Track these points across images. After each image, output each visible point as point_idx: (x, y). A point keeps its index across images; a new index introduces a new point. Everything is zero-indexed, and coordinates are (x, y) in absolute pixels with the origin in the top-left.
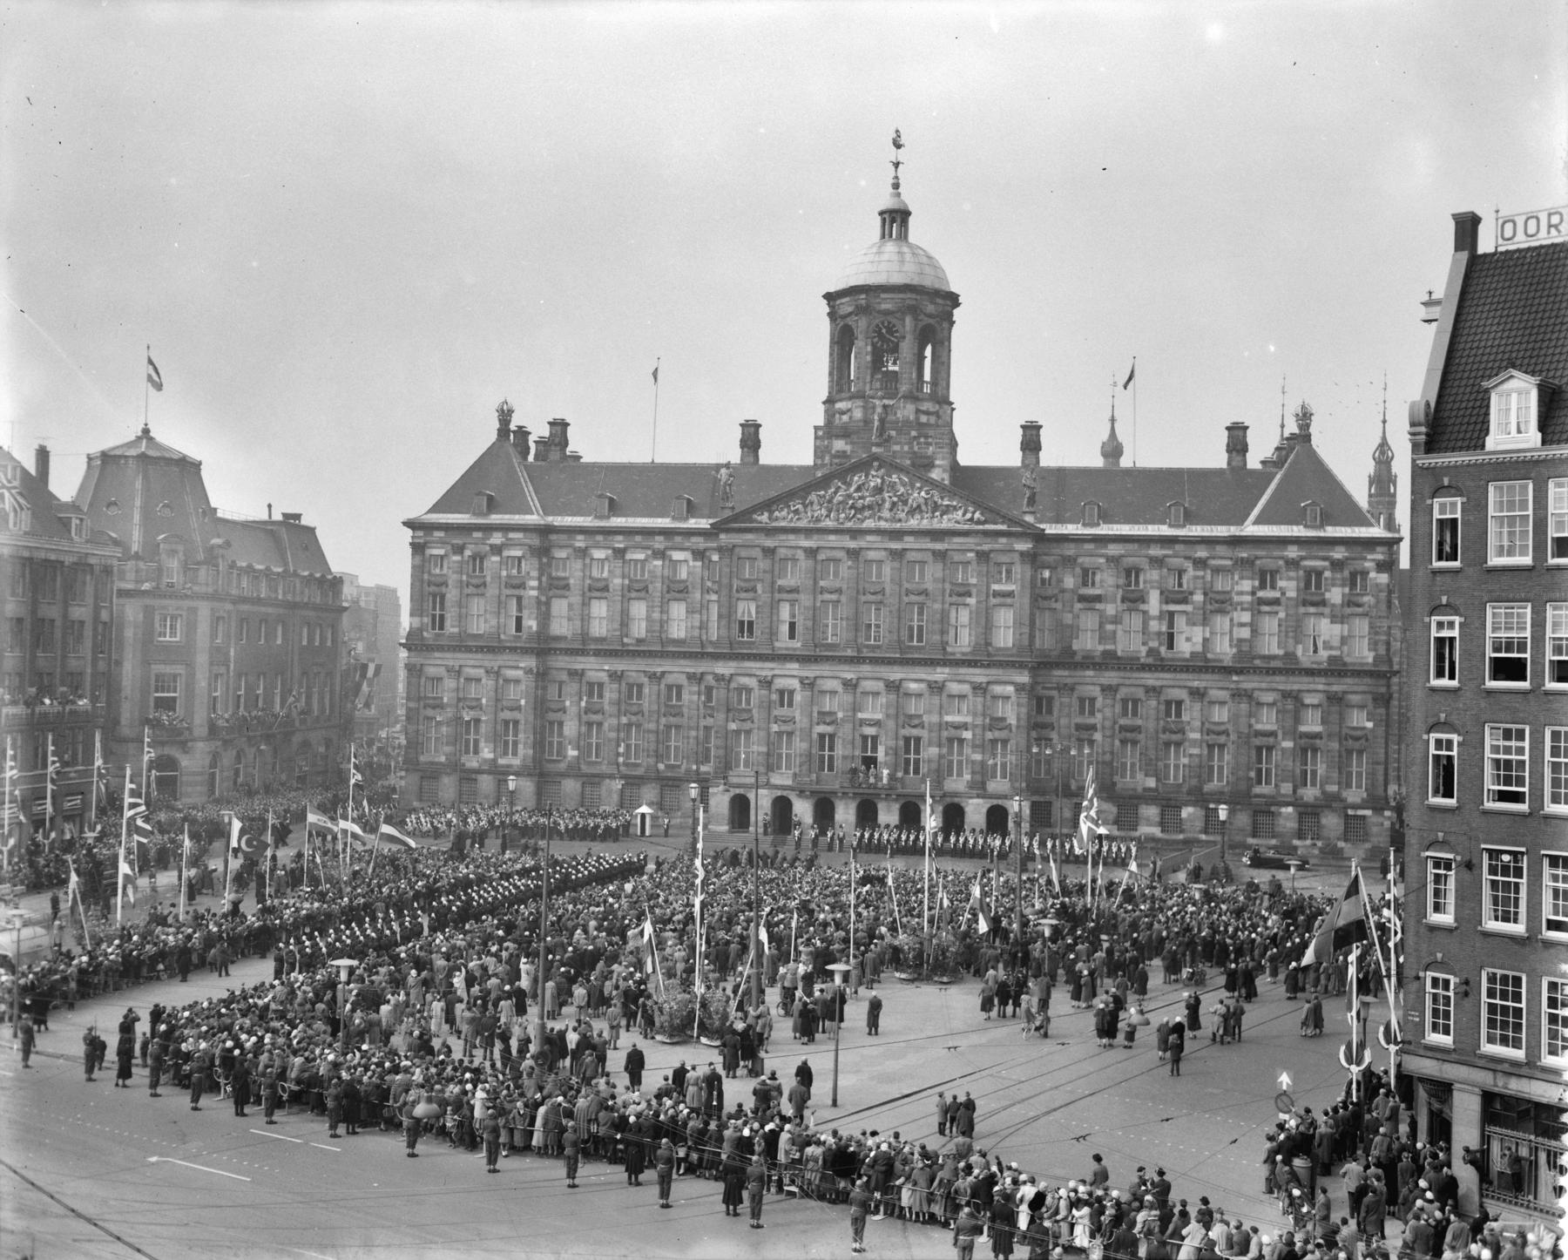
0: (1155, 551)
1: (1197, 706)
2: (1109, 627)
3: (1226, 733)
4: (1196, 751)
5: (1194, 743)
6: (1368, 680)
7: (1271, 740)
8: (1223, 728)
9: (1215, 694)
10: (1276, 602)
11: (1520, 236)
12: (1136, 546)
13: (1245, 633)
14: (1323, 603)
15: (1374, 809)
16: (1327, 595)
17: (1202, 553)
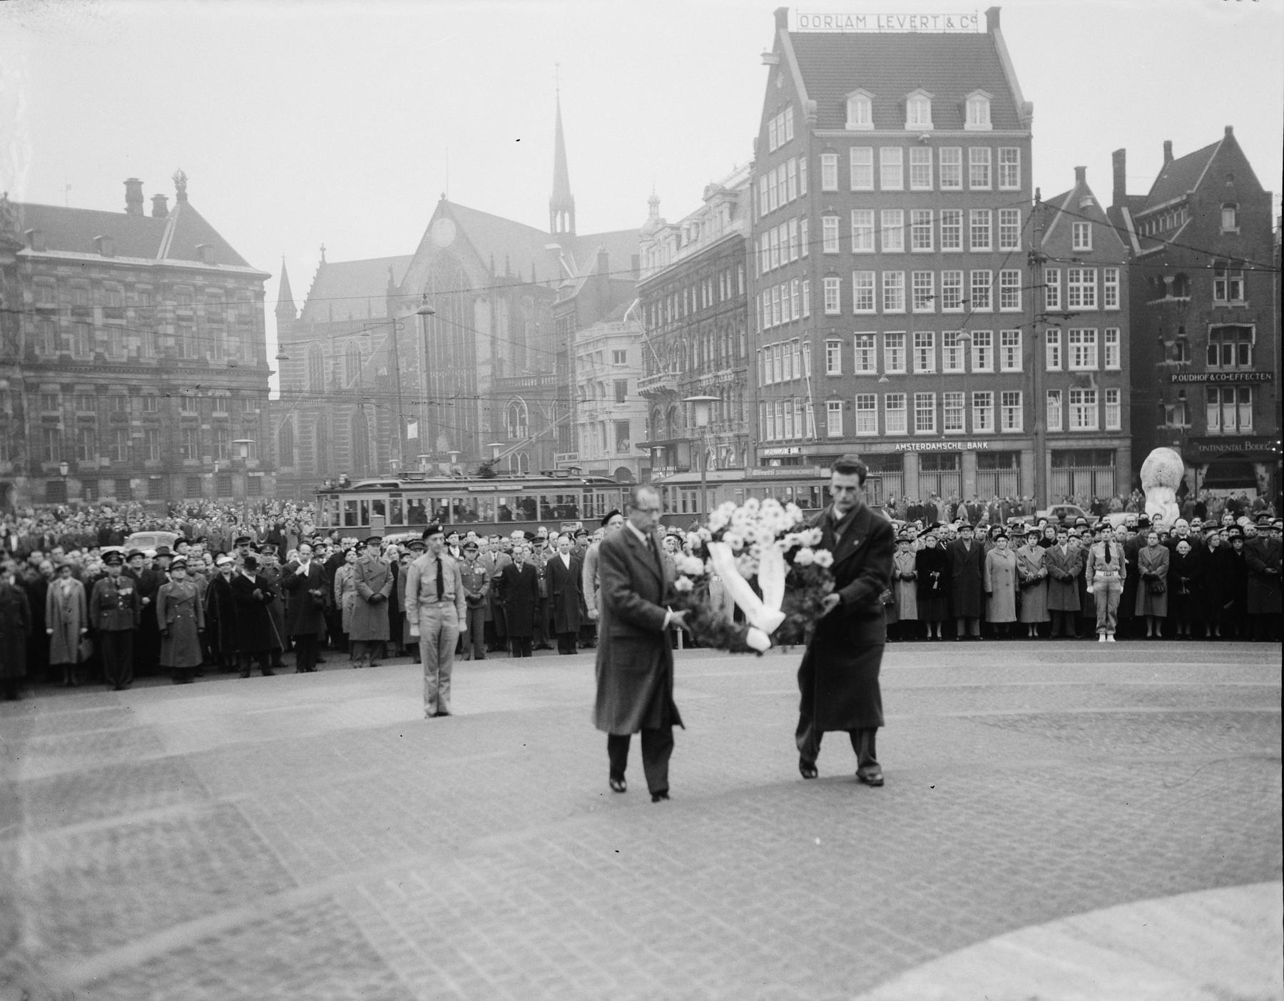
0: (95, 274)
1: (135, 400)
2: (64, 336)
3: (158, 420)
4: (136, 435)
5: (137, 429)
6: (255, 379)
7: (194, 424)
8: (155, 416)
9: (146, 390)
10: (190, 319)
11: (811, 26)
12: (79, 270)
13: (171, 342)
14: (221, 321)
15: (265, 471)
16: (224, 315)
17: (130, 278)
